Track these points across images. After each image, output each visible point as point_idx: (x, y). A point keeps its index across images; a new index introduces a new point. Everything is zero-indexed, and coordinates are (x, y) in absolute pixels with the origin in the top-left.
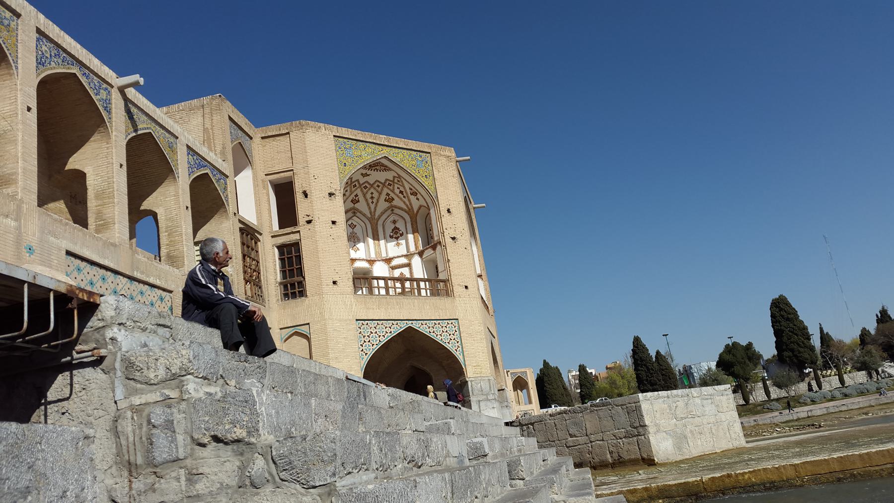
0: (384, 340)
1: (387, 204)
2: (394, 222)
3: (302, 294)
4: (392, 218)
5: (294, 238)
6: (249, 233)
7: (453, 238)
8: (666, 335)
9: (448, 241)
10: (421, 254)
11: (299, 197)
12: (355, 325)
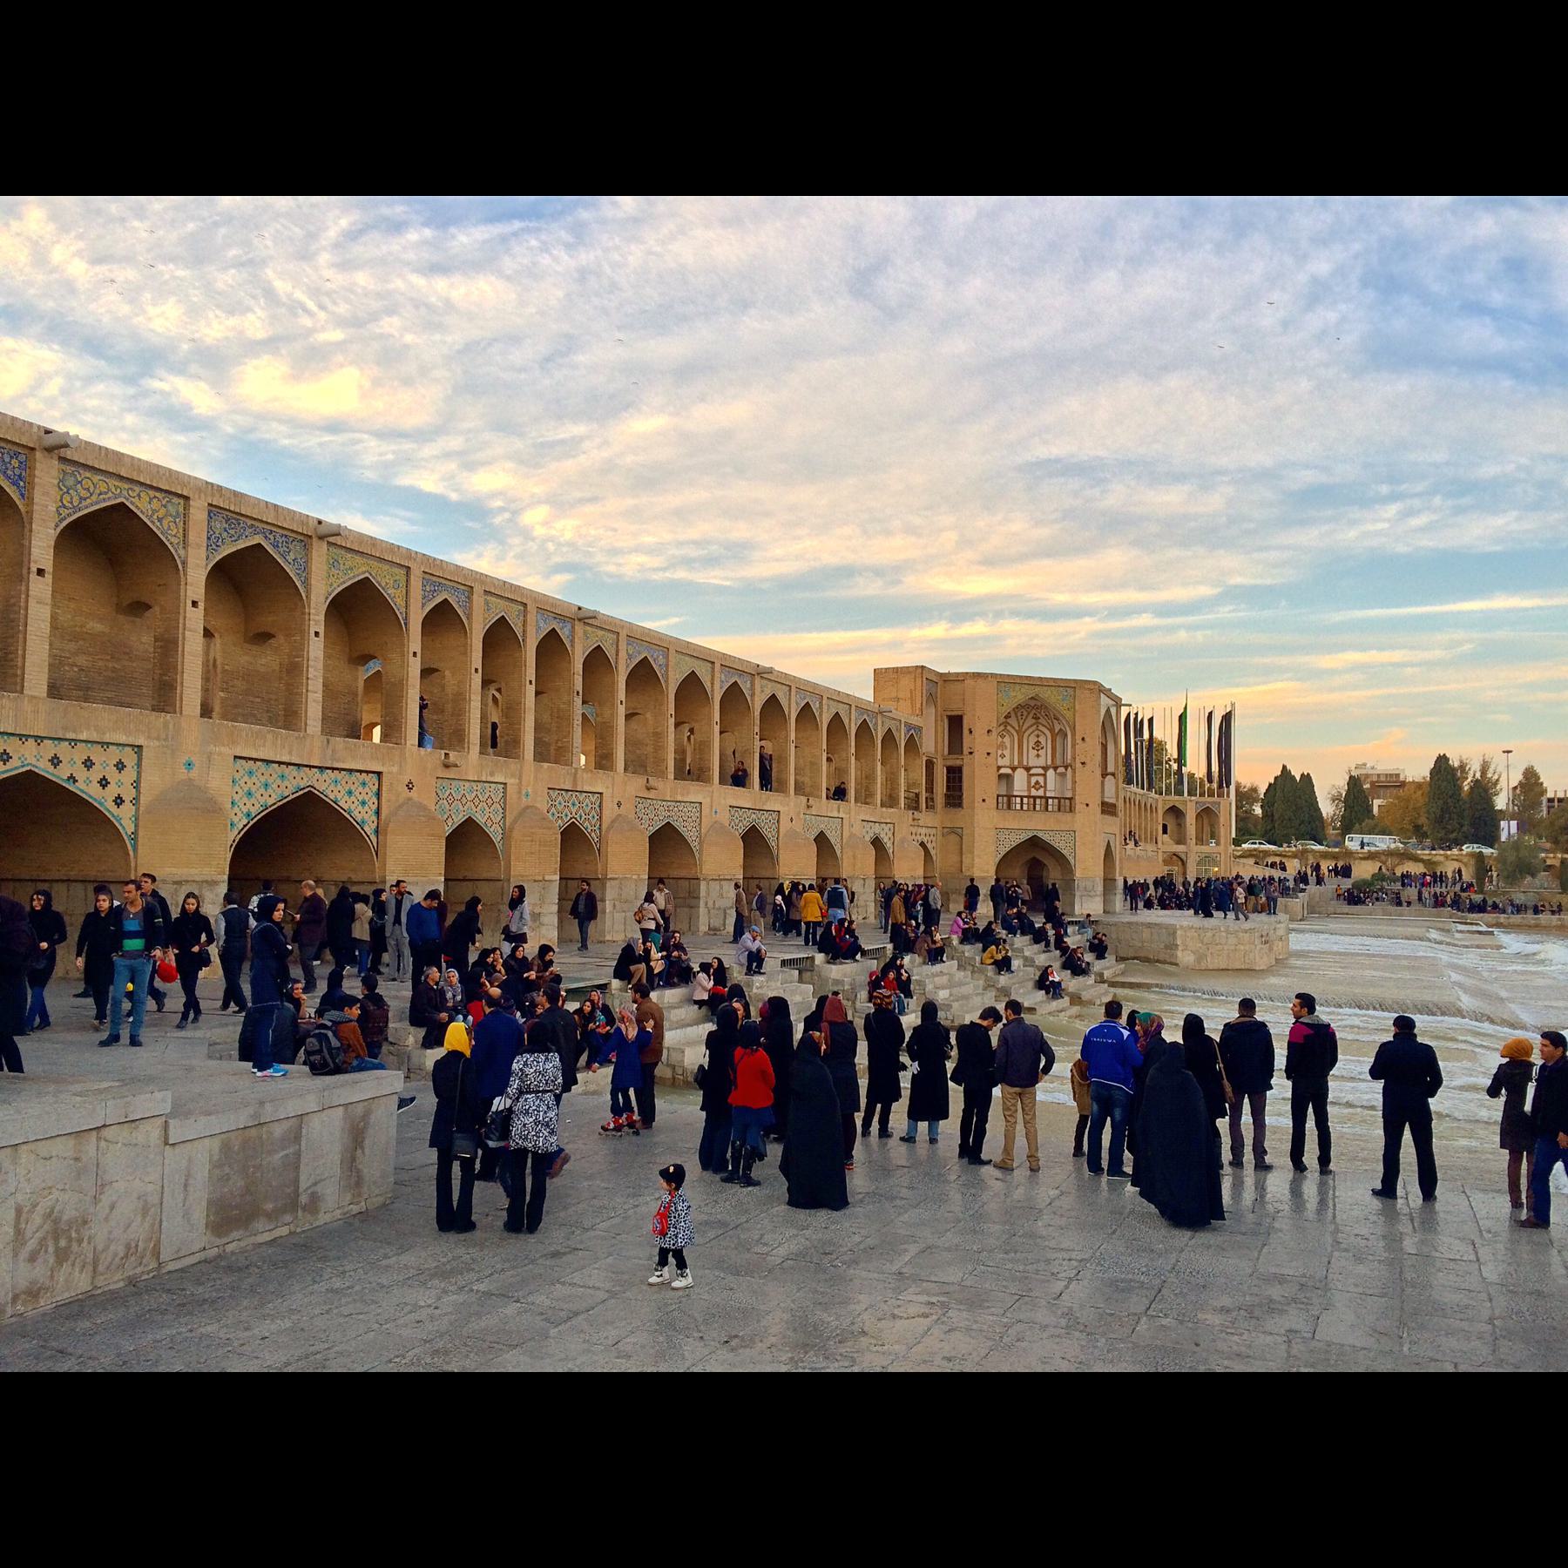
0: (1014, 844)
1: (1034, 721)
2: (1038, 736)
3: (960, 805)
4: (1036, 732)
5: (958, 763)
6: (930, 765)
7: (1083, 763)
8: (1509, 752)
9: (1078, 765)
10: (1055, 768)
11: (966, 732)
12: (993, 832)
